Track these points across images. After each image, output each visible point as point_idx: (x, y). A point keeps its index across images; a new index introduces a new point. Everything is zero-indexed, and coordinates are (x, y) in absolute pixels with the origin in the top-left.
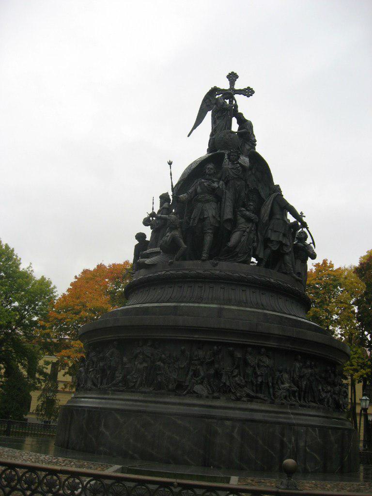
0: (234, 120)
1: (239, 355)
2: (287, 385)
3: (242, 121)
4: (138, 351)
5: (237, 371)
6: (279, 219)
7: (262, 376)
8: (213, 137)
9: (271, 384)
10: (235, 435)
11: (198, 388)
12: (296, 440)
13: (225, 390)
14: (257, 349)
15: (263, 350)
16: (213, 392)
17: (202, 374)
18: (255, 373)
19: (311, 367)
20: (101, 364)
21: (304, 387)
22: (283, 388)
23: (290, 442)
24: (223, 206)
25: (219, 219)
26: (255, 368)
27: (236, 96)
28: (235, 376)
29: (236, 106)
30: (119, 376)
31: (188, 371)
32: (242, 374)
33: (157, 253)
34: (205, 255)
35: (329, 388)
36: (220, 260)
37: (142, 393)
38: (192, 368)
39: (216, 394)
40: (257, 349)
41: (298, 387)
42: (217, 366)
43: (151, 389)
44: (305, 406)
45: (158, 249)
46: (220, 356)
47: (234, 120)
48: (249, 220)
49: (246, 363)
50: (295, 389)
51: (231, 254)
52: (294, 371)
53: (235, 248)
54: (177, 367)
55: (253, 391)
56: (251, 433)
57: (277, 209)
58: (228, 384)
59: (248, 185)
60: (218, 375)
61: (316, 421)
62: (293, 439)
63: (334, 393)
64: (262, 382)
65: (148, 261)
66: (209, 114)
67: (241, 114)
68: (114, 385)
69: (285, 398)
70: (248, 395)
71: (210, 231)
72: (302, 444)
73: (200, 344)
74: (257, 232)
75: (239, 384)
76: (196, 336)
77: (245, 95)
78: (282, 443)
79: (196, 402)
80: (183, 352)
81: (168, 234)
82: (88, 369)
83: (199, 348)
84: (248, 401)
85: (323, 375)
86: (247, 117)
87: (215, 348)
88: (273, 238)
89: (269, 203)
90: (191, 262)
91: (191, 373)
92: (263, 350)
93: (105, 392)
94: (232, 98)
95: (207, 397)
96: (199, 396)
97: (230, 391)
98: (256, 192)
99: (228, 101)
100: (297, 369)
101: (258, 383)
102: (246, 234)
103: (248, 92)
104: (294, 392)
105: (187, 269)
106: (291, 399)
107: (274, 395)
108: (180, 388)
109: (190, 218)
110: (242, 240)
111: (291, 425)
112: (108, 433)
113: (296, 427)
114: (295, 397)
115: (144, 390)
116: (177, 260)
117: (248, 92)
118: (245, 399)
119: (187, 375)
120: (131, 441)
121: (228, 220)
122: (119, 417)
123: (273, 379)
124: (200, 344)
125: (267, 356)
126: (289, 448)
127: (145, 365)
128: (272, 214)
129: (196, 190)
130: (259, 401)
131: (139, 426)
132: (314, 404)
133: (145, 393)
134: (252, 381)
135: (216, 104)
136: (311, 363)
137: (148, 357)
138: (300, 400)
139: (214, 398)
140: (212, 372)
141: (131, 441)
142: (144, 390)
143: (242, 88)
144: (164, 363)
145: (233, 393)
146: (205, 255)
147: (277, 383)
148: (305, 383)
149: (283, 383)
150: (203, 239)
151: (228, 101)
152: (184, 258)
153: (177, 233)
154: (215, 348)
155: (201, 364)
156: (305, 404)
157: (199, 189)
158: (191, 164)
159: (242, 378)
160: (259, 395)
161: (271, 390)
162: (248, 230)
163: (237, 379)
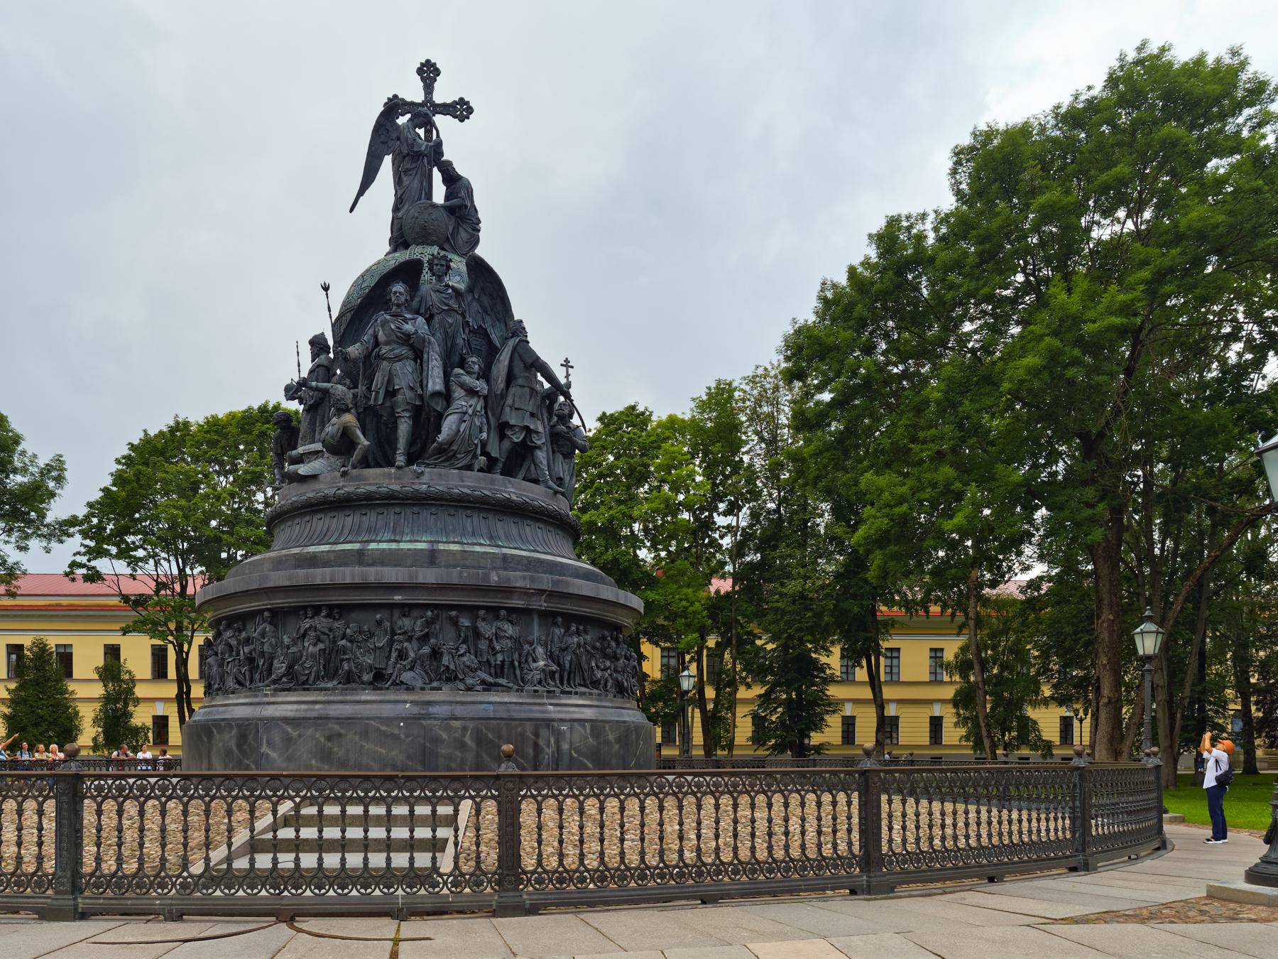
0: (437, 176)
1: (465, 622)
2: (542, 663)
3: (452, 179)
4: (307, 626)
5: (465, 646)
6: (522, 386)
7: (502, 651)
8: (400, 215)
9: (516, 664)
10: (468, 740)
11: (407, 676)
12: (557, 742)
13: (451, 677)
14: (494, 611)
15: (503, 613)
16: (431, 681)
17: (412, 655)
18: (493, 649)
19: (578, 633)
20: (247, 649)
21: (567, 665)
22: (536, 669)
23: (548, 746)
24: (425, 368)
25: (420, 391)
26: (491, 641)
27: (439, 120)
28: (462, 655)
29: (439, 144)
30: (280, 667)
31: (390, 652)
32: (472, 652)
33: (317, 453)
34: (400, 459)
35: (608, 664)
36: (427, 465)
37: (322, 689)
38: (396, 646)
39: (435, 684)
40: (494, 611)
41: (559, 665)
42: (432, 641)
43: (335, 682)
44: (570, 693)
45: (318, 446)
46: (437, 627)
47: (437, 176)
48: (471, 392)
49: (477, 635)
50: (554, 668)
51: (446, 455)
52: (552, 641)
53: (451, 444)
54: (372, 646)
55: (491, 675)
56: (490, 736)
57: (519, 367)
58: (452, 667)
59: (468, 322)
60: (436, 654)
61: (589, 713)
62: (552, 742)
63: (616, 671)
64: (503, 661)
65: (303, 469)
66: (388, 160)
67: (449, 163)
68: (275, 682)
69: (540, 682)
70: (483, 682)
71: (407, 414)
72: (565, 746)
73: (406, 609)
74: (486, 412)
75: (468, 667)
76: (398, 598)
77: (455, 117)
78: (536, 746)
79: (405, 697)
80: (379, 623)
81: (334, 420)
82: (223, 659)
83: (404, 616)
84: (484, 690)
85: (598, 644)
86: (461, 169)
87: (429, 613)
88: (512, 422)
89: (504, 357)
90: (378, 471)
91: (394, 655)
92: (503, 613)
93: (255, 691)
94: (429, 125)
95: (423, 689)
96: (410, 689)
97: (456, 677)
98: (483, 333)
99: (421, 132)
100: (556, 639)
101: (498, 662)
102: (467, 417)
103: (461, 110)
104: (552, 674)
105: (374, 484)
106: (548, 684)
107: (522, 679)
108: (379, 679)
109: (369, 388)
110: (462, 430)
111: (548, 722)
112: (274, 755)
113: (556, 724)
114: (553, 679)
115: (323, 685)
116: (354, 467)
117: (461, 110)
118: (479, 688)
119: (389, 657)
120: (314, 762)
121: (436, 394)
122: (289, 730)
123: (520, 655)
124: (406, 609)
125: (511, 622)
126: (548, 754)
127: (321, 646)
128: (510, 378)
129: (376, 337)
130: (500, 688)
131: (322, 740)
132: (583, 689)
133: (326, 689)
134: (488, 660)
135: (398, 139)
136: (577, 629)
137: (325, 634)
138: (562, 683)
139: (432, 689)
140: (426, 650)
141: (314, 762)
142: (323, 685)
143: (449, 101)
144: (351, 642)
145: (461, 680)
146: (400, 459)
147: (526, 661)
148: (569, 658)
149: (535, 661)
150: (395, 428)
151: (421, 132)
152: (365, 463)
153: (349, 418)
154: (429, 613)
155: (410, 639)
156: (570, 689)
157: (381, 335)
158: (362, 276)
159: (473, 657)
160: (501, 681)
161: (518, 672)
162: (470, 411)
163: (465, 659)
